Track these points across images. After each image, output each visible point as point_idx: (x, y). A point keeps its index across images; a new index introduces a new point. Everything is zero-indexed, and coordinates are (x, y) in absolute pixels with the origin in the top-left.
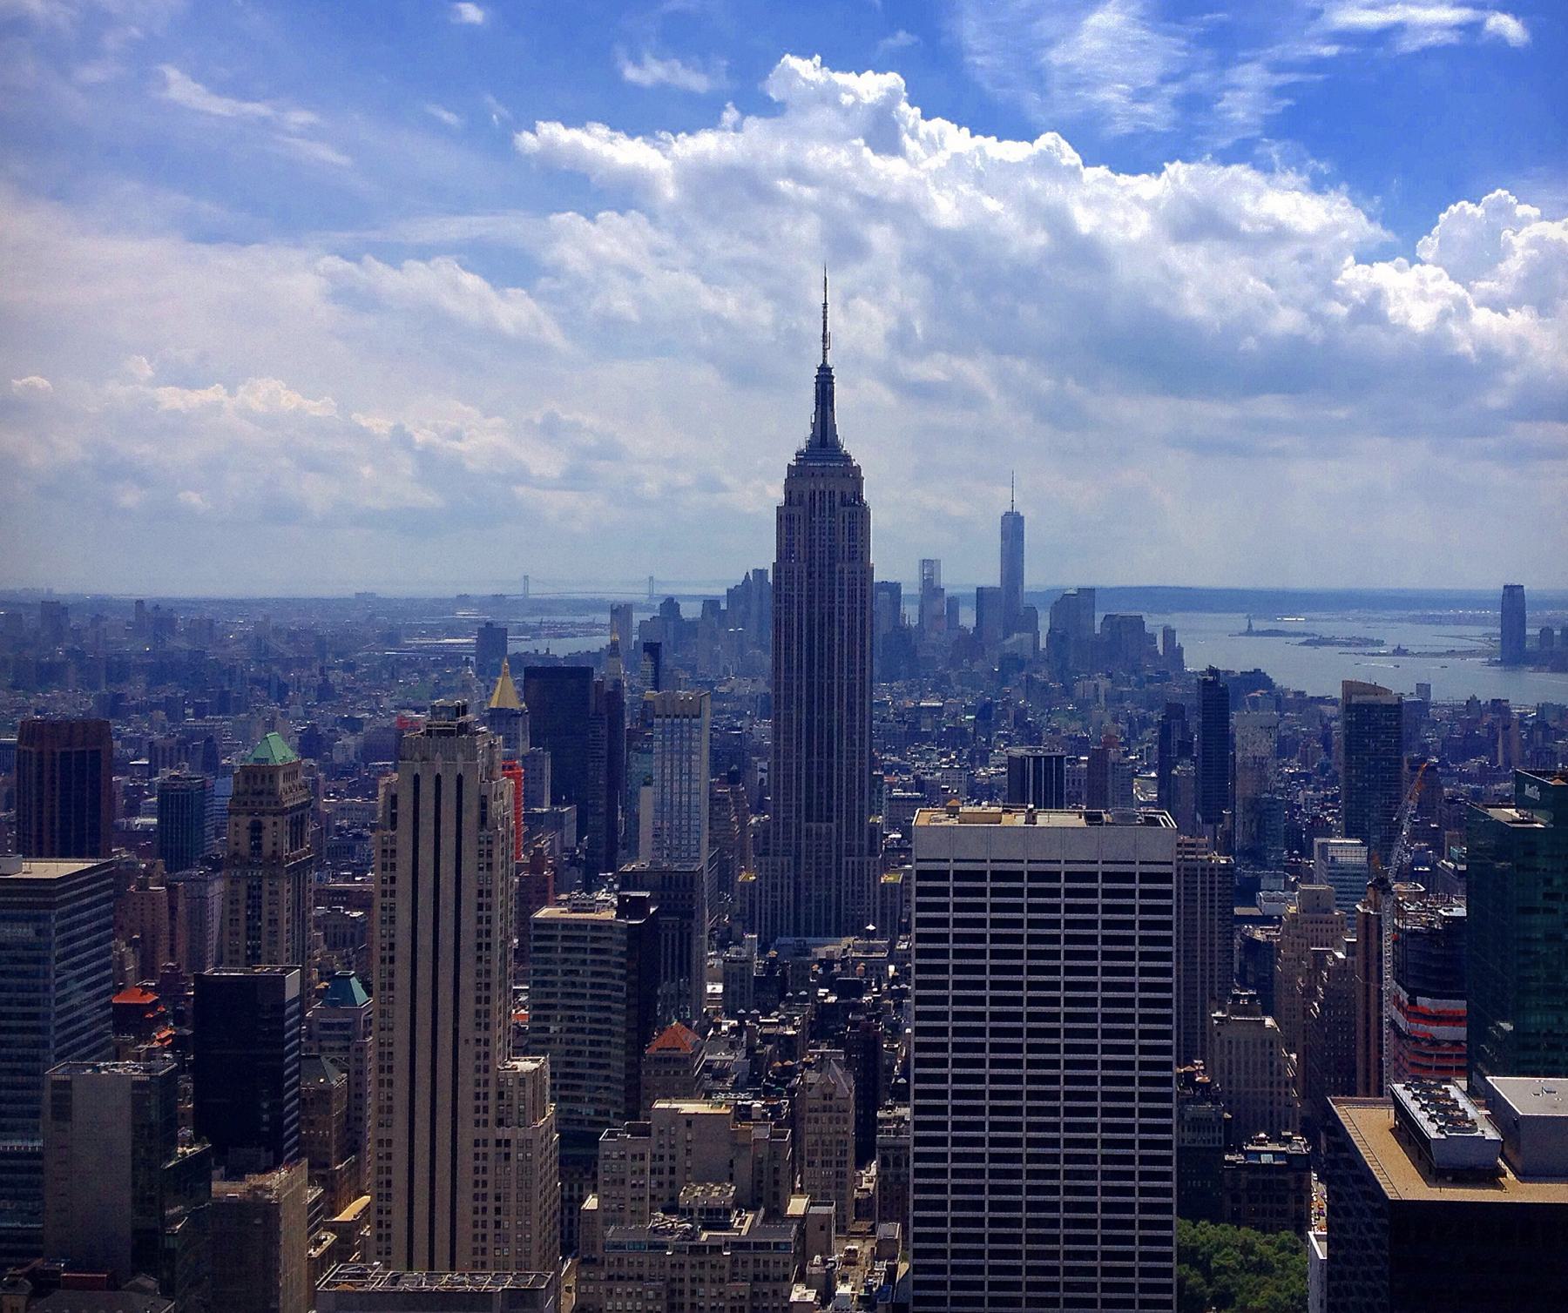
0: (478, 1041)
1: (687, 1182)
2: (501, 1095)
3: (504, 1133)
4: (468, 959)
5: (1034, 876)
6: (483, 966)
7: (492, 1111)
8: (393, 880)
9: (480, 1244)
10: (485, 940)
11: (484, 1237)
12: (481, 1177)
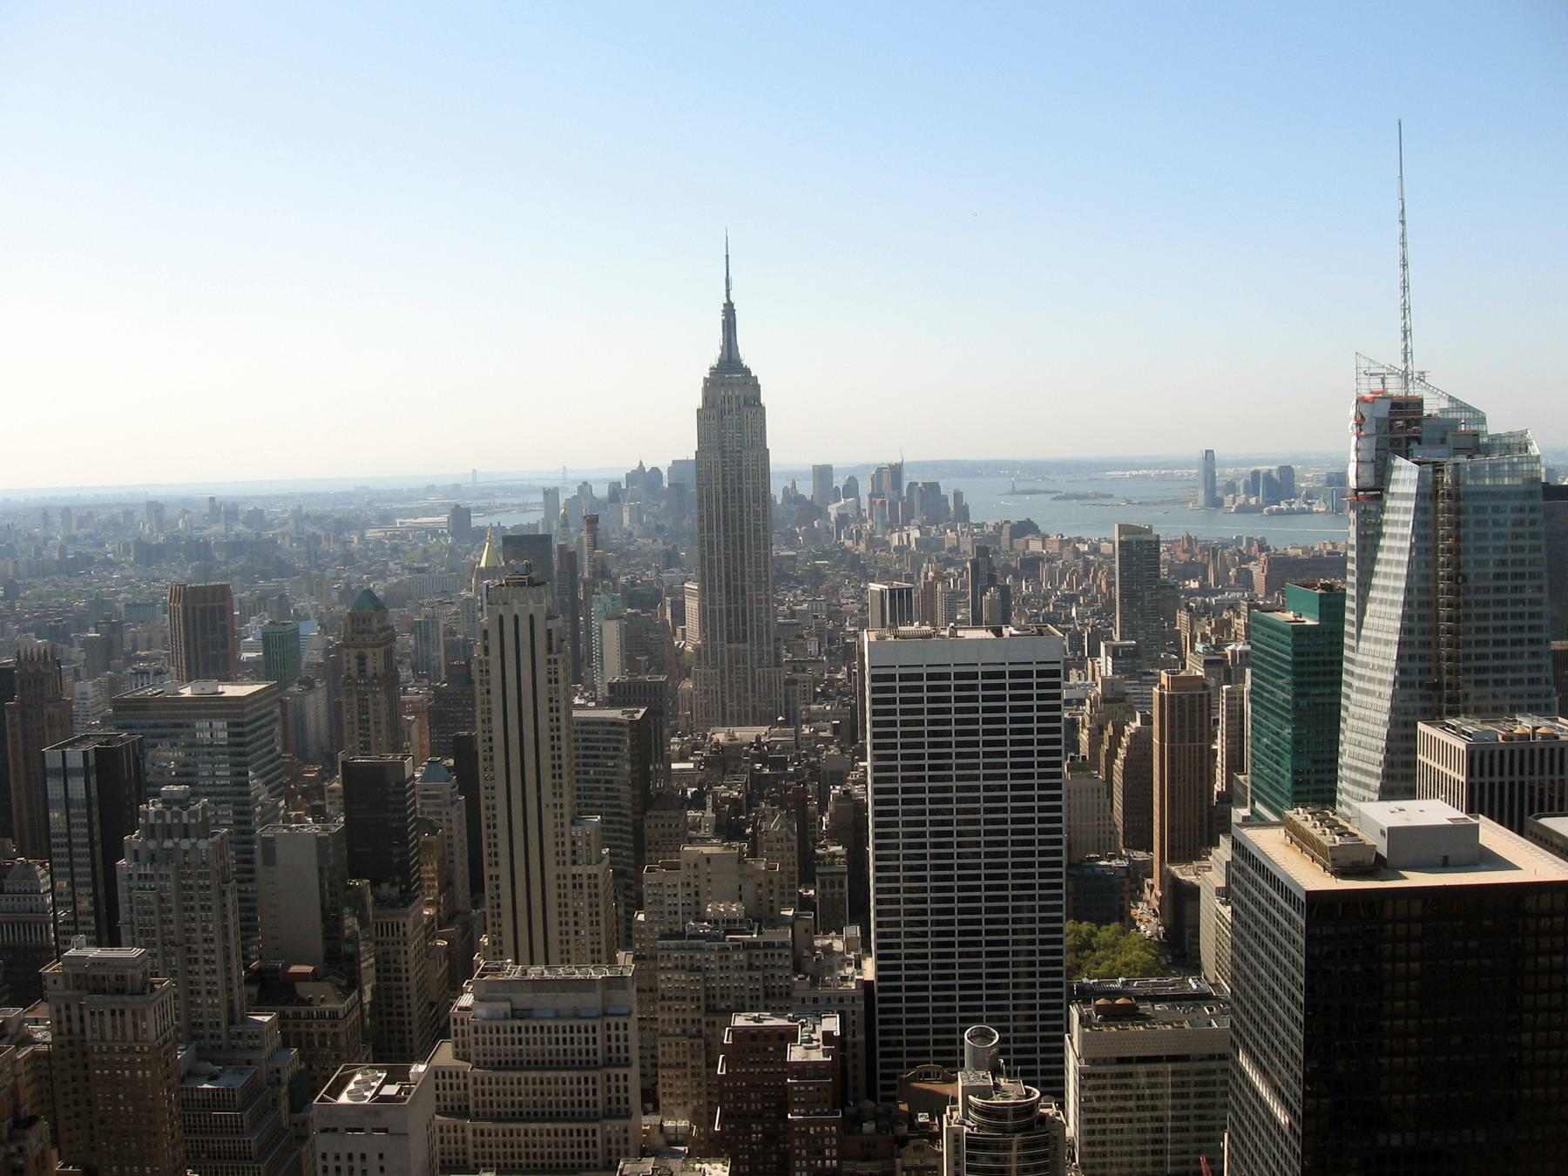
0: (555, 805)
1: (709, 902)
2: (574, 843)
3: (576, 870)
4: (545, 749)
5: (959, 676)
6: (556, 752)
7: (568, 853)
8: (488, 692)
9: (565, 947)
10: (555, 734)
11: (568, 942)
12: (562, 900)
